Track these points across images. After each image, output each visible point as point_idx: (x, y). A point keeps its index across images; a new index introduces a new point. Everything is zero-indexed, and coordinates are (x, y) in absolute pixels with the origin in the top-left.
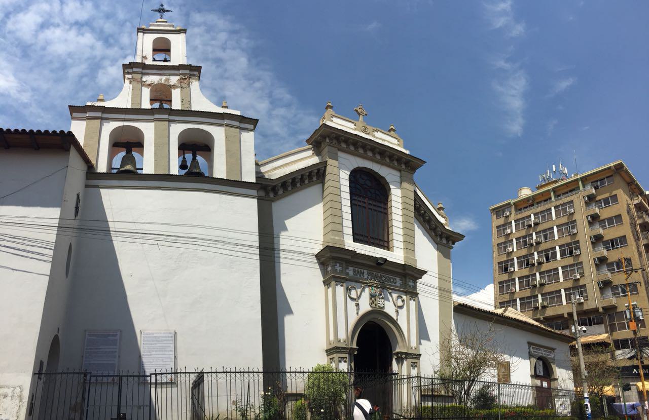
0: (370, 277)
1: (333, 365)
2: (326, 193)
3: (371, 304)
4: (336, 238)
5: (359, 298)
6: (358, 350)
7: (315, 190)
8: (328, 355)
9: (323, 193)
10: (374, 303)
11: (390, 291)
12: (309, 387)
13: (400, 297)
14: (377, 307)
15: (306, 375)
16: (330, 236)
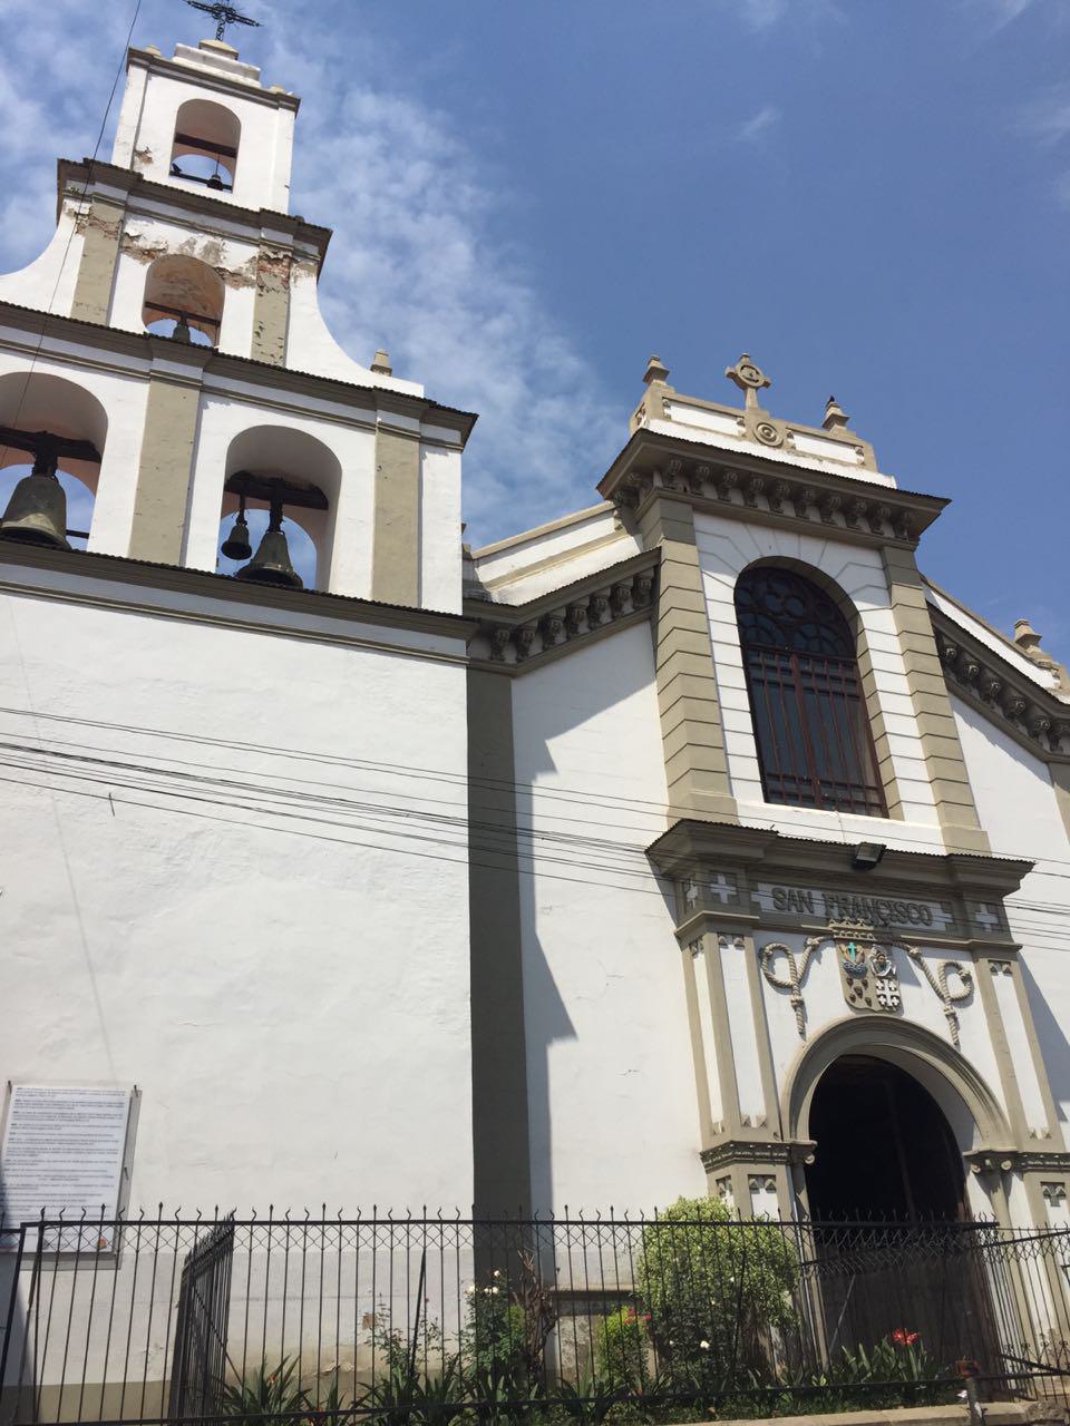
0: (835, 912)
1: (729, 1201)
2: (663, 653)
3: (853, 999)
4: (708, 793)
5: (802, 981)
6: (816, 1151)
7: (627, 645)
8: (709, 1169)
9: (655, 651)
10: (860, 995)
11: (914, 950)
12: (648, 1270)
13: (953, 967)
14: (876, 1007)
15: (636, 1232)
16: (688, 788)
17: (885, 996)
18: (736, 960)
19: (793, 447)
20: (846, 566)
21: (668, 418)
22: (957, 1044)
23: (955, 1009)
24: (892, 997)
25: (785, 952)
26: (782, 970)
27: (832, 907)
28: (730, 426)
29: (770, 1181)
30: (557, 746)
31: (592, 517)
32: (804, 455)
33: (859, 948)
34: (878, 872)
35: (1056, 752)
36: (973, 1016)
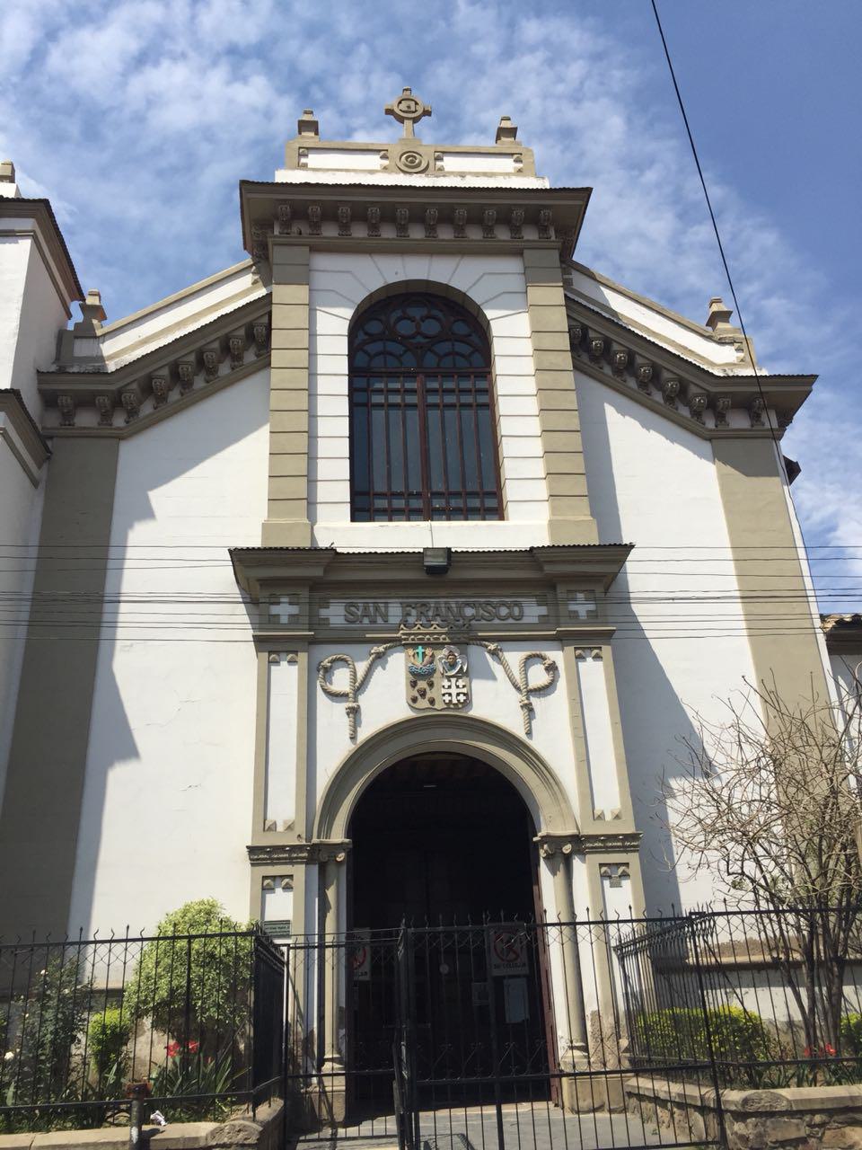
3: (414, 700)
11: (492, 647)
17: (450, 695)
18: (287, 676)
19: (441, 169)
20: (484, 274)
21: (305, 166)
22: (529, 733)
23: (533, 700)
24: (458, 694)
25: (343, 661)
26: (341, 680)
27: (409, 615)
28: (374, 161)
29: (287, 880)
30: (157, 497)
31: (226, 278)
32: (452, 173)
33: (429, 652)
34: (453, 575)
35: (720, 428)
36: (555, 709)
